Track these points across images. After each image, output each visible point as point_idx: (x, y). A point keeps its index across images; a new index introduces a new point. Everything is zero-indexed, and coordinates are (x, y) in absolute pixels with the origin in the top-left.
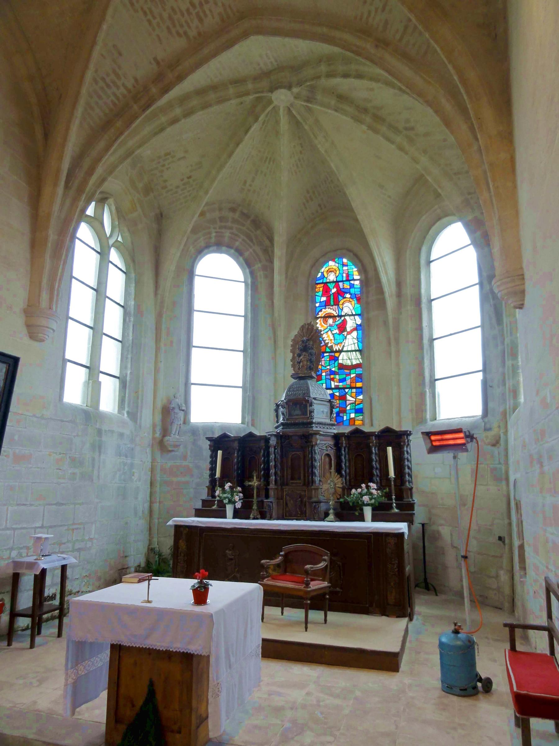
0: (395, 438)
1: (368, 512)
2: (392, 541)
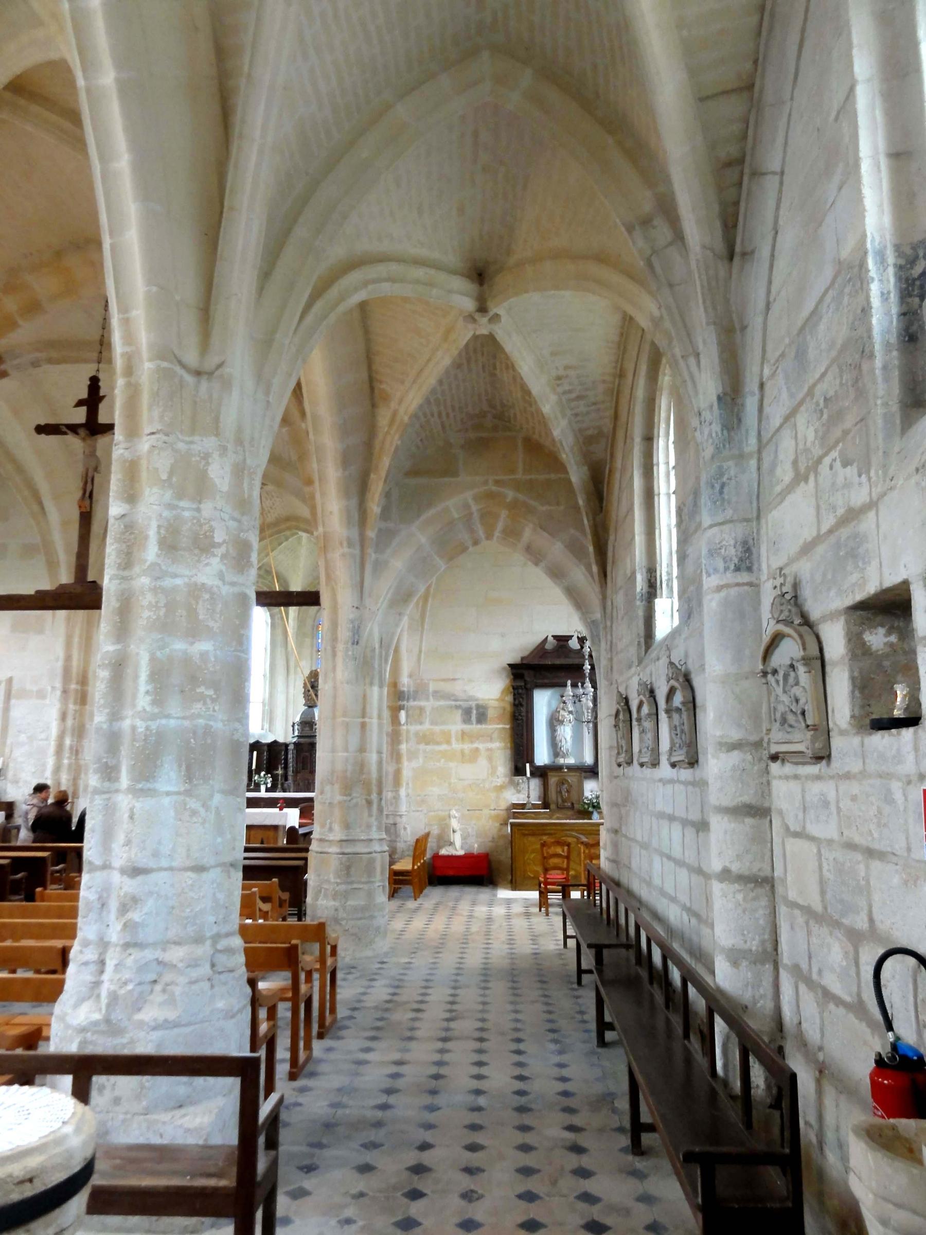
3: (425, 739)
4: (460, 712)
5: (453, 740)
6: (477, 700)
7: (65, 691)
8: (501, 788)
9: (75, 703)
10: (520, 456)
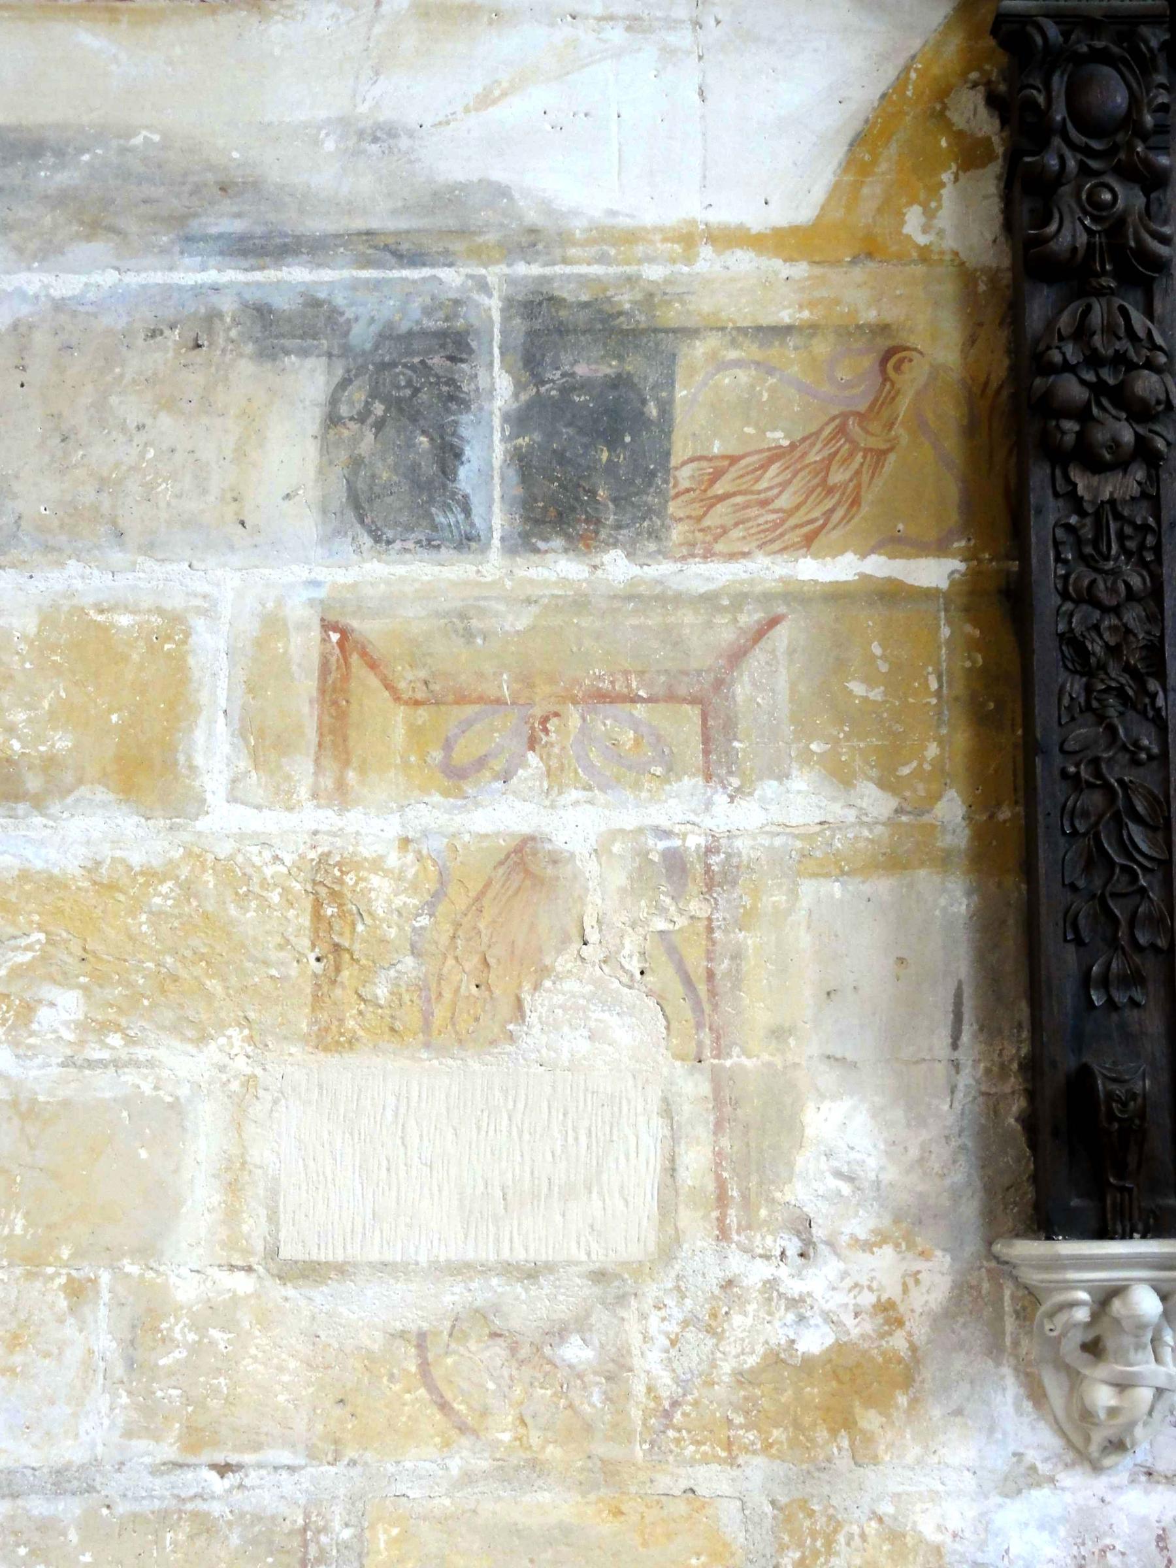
4: (310, 380)
5: (213, 750)
6: (531, 242)
8: (852, 1391)
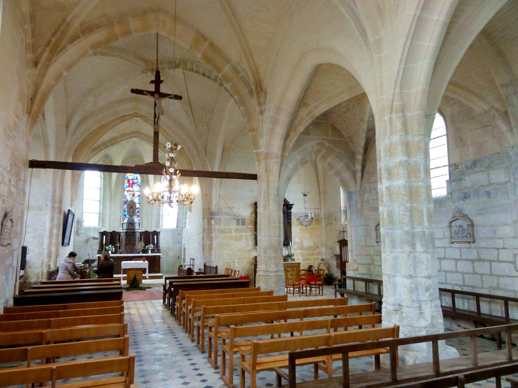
0: (156, 233)
1: (150, 251)
2: (157, 257)
3: (222, 231)
4: (235, 220)
5: (233, 232)
7: (53, 207)
8: (250, 251)
9: (58, 213)
10: (330, 130)
